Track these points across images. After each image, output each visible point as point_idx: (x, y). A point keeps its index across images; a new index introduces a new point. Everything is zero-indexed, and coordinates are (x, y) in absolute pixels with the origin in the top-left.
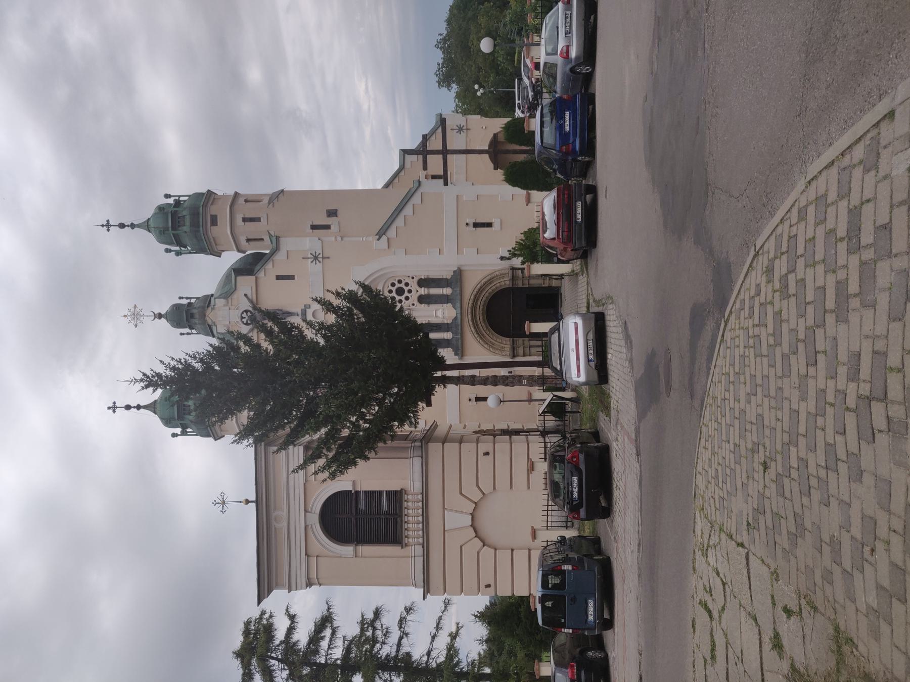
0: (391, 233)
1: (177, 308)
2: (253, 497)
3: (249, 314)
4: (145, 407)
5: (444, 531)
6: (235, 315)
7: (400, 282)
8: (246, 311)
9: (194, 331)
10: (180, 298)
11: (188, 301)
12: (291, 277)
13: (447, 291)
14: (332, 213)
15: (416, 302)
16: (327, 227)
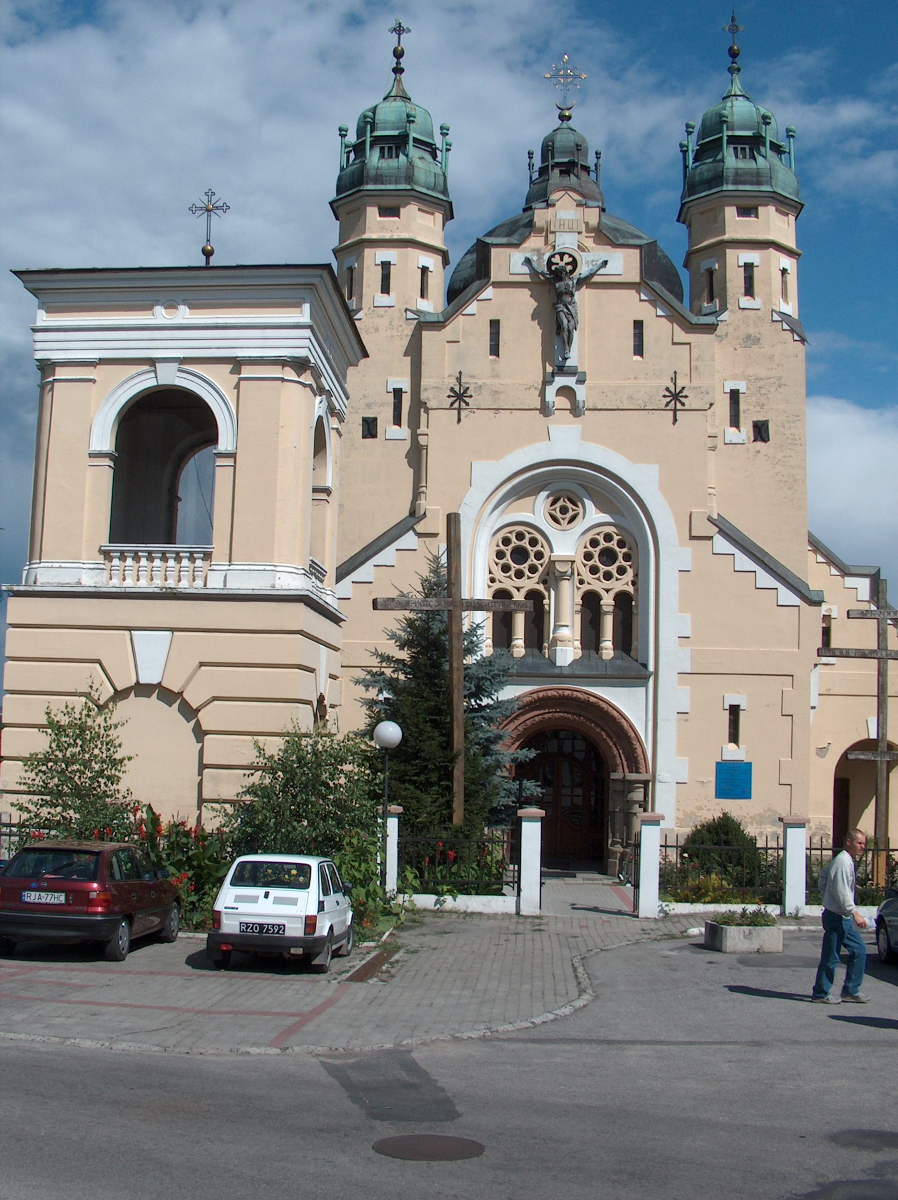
0: (721, 544)
2: (214, 261)
3: (569, 268)
5: (130, 629)
6: (566, 241)
8: (574, 263)
9: (536, 176)
11: (593, 168)
12: (639, 350)
14: (761, 431)
15: (585, 588)
16: (735, 421)
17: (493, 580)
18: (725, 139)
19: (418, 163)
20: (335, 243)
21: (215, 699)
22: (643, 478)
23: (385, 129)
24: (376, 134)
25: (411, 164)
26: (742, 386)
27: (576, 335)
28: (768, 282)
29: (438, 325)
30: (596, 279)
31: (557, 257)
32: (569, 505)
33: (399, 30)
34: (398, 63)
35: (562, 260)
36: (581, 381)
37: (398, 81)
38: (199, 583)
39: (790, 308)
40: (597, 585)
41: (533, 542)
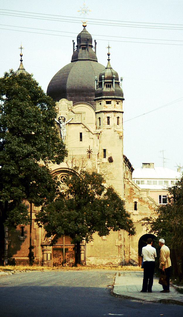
1: (89, 40)
9: (76, 48)
10: (95, 41)
12: (81, 140)
16: (105, 157)
31: (61, 117)
35: (62, 118)
37: (21, 63)
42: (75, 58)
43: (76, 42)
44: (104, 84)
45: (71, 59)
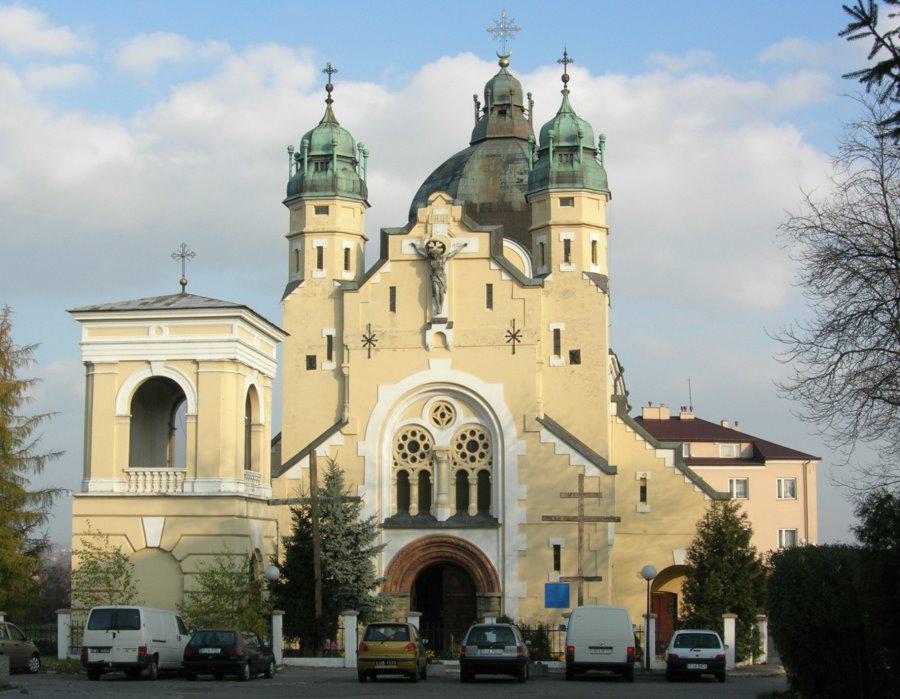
1: (514, 91)
4: (329, 110)
5: (142, 516)
6: (440, 232)
7: (486, 446)
8: (444, 247)
9: (481, 114)
10: (529, 95)
12: (490, 305)
13: (473, 508)
14: (575, 357)
15: (458, 468)
17: (396, 464)
18: (551, 149)
19: (341, 174)
20: (287, 231)
21: (190, 554)
22: (493, 393)
23: (317, 149)
24: (312, 153)
25: (335, 177)
26: (562, 327)
27: (446, 297)
28: (580, 252)
29: (356, 290)
30: (456, 257)
32: (446, 411)
33: (329, 71)
34: (329, 96)
36: (450, 326)
38: (179, 489)
39: (599, 269)
40: (466, 466)
41: (423, 437)
42: (478, 139)
43: (482, 100)
44: (554, 151)
45: (469, 139)
